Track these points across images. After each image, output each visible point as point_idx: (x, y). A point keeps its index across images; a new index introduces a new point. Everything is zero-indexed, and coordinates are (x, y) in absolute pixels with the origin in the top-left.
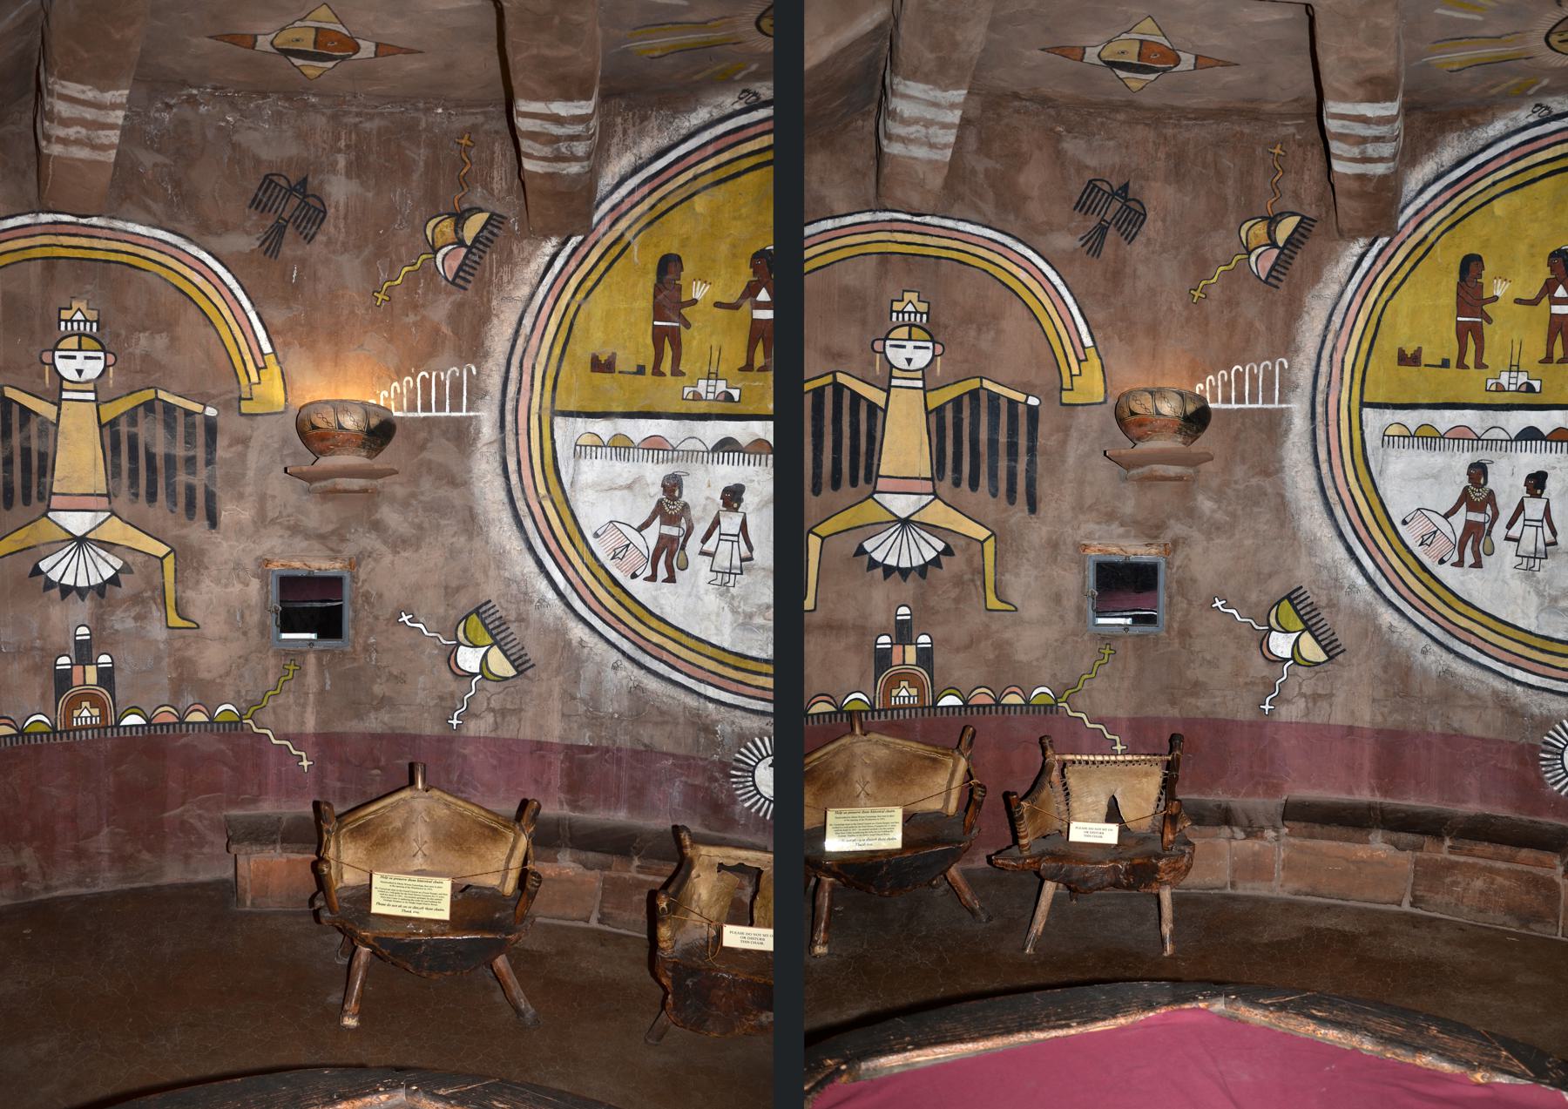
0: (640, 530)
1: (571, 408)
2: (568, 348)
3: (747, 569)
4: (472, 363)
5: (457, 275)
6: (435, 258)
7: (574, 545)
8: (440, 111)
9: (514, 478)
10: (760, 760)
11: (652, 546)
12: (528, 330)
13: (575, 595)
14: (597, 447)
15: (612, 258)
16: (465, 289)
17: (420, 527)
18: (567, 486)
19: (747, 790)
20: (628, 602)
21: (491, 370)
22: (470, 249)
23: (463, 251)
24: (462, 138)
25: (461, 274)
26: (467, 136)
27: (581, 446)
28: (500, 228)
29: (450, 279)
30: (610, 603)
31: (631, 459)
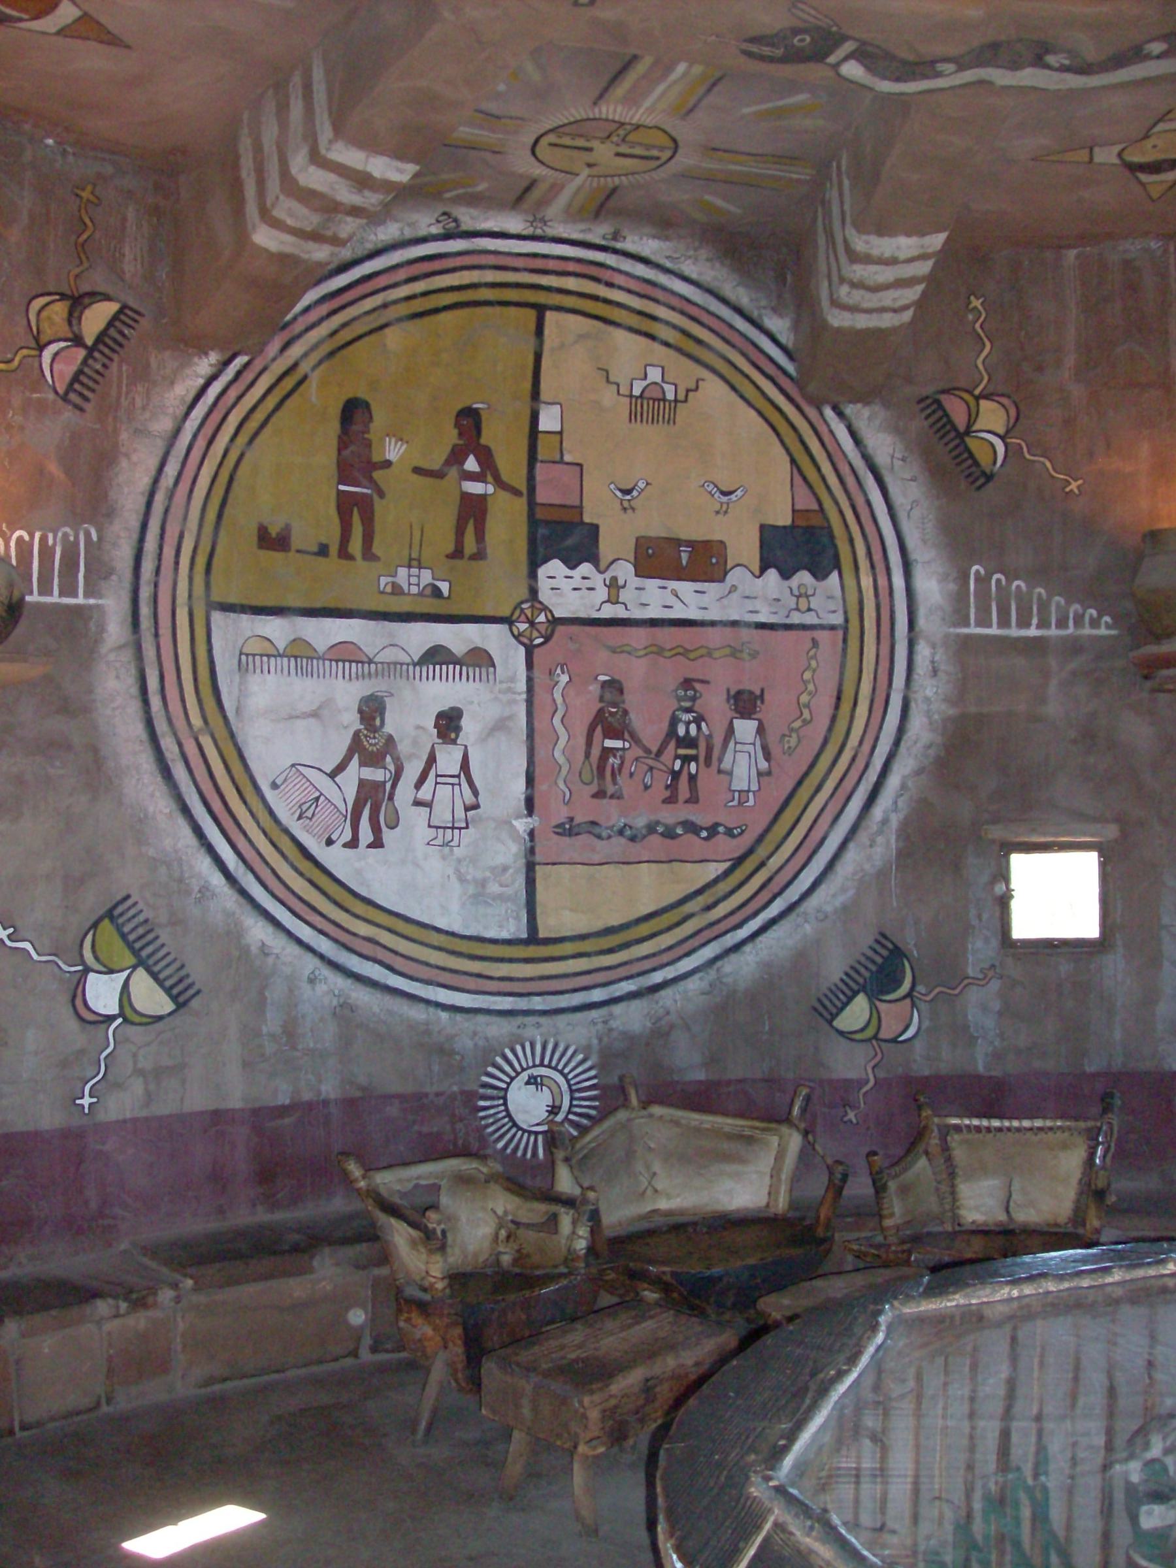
0: (333, 775)
1: (232, 600)
2: (228, 510)
3: (473, 820)
4: (90, 522)
5: (70, 388)
6: (40, 356)
7: (245, 802)
8: (50, 141)
9: (155, 702)
10: (512, 1079)
11: (351, 796)
12: (171, 481)
13: (250, 877)
14: (269, 656)
15: (284, 392)
16: (81, 410)
17: (20, 780)
18: (231, 714)
19: (499, 1124)
20: (323, 881)
21: (119, 537)
22: (91, 351)
23: (81, 353)
24: (83, 189)
25: (77, 386)
26: (89, 188)
27: (247, 655)
28: (133, 328)
29: (61, 391)
30: (299, 885)
31: (315, 675)
